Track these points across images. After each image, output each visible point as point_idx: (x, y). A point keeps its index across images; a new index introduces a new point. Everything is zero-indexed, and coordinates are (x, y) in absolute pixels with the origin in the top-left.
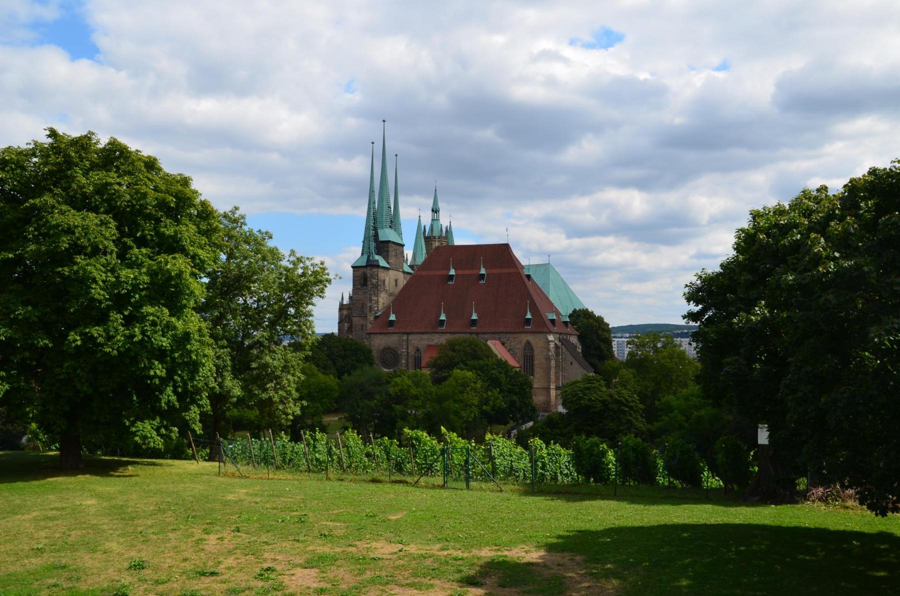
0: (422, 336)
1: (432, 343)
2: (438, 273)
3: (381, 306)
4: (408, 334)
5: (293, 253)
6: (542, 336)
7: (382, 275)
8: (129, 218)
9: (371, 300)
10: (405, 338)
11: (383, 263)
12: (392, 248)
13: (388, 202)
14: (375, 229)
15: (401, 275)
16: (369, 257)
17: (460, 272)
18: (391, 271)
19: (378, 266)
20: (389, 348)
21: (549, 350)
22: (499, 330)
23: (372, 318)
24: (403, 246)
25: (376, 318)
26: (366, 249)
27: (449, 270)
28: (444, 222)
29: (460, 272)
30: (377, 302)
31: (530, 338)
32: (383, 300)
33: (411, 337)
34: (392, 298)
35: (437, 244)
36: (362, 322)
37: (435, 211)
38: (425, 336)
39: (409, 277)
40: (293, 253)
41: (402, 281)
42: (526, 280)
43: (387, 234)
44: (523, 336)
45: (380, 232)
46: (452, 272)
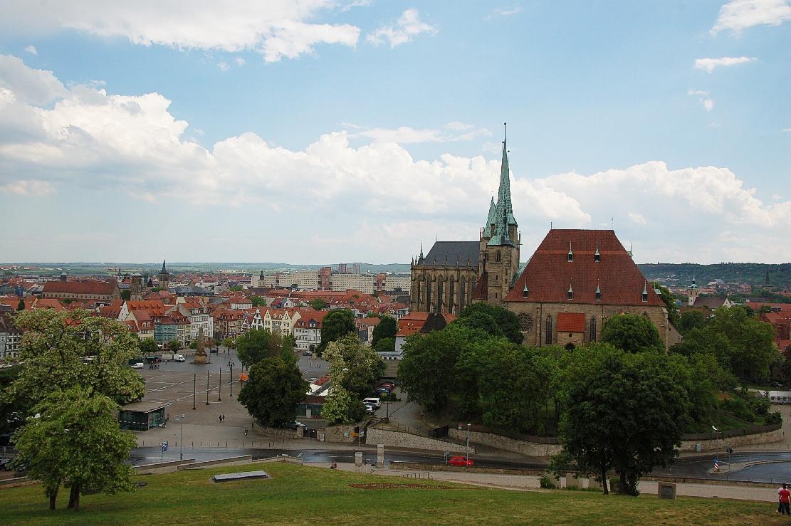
0: (553, 305)
1: (562, 312)
2: (560, 252)
4: (542, 303)
6: (657, 309)
10: (539, 305)
16: (503, 239)
17: (576, 253)
19: (512, 246)
20: (524, 314)
21: (665, 321)
22: (621, 303)
23: (507, 289)
25: (511, 288)
29: (576, 253)
31: (648, 310)
33: (544, 306)
36: (497, 291)
38: (555, 305)
44: (641, 308)
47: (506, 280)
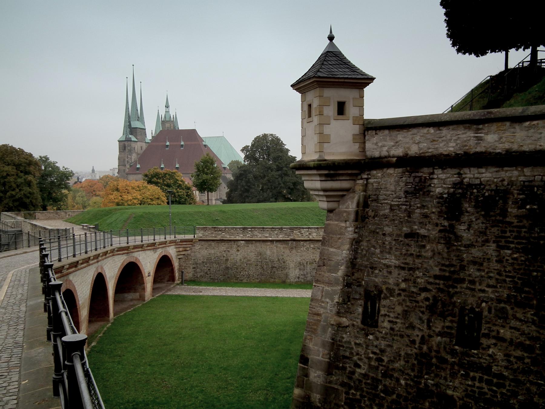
2: (161, 144)
3: (133, 160)
5: (64, 167)
7: (133, 145)
8: (18, 166)
9: (128, 157)
11: (134, 139)
12: (138, 130)
13: (137, 107)
14: (129, 122)
15: (144, 144)
17: (172, 143)
18: (138, 143)
19: (131, 141)
24: (145, 129)
25: (131, 166)
26: (125, 132)
27: (166, 142)
28: (172, 113)
29: (172, 143)
30: (131, 159)
32: (134, 157)
34: (139, 156)
35: (167, 125)
37: (167, 107)
39: (147, 144)
40: (64, 167)
41: (145, 146)
42: (203, 148)
43: (136, 124)
45: (132, 122)
46: (168, 143)
47: (128, 161)
